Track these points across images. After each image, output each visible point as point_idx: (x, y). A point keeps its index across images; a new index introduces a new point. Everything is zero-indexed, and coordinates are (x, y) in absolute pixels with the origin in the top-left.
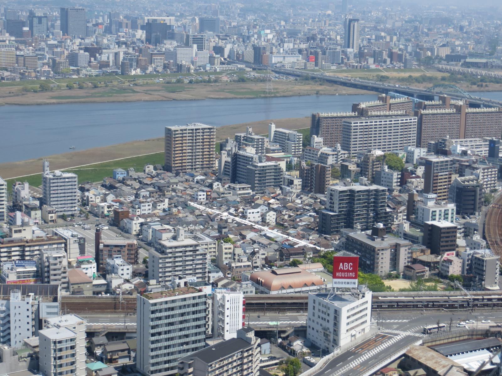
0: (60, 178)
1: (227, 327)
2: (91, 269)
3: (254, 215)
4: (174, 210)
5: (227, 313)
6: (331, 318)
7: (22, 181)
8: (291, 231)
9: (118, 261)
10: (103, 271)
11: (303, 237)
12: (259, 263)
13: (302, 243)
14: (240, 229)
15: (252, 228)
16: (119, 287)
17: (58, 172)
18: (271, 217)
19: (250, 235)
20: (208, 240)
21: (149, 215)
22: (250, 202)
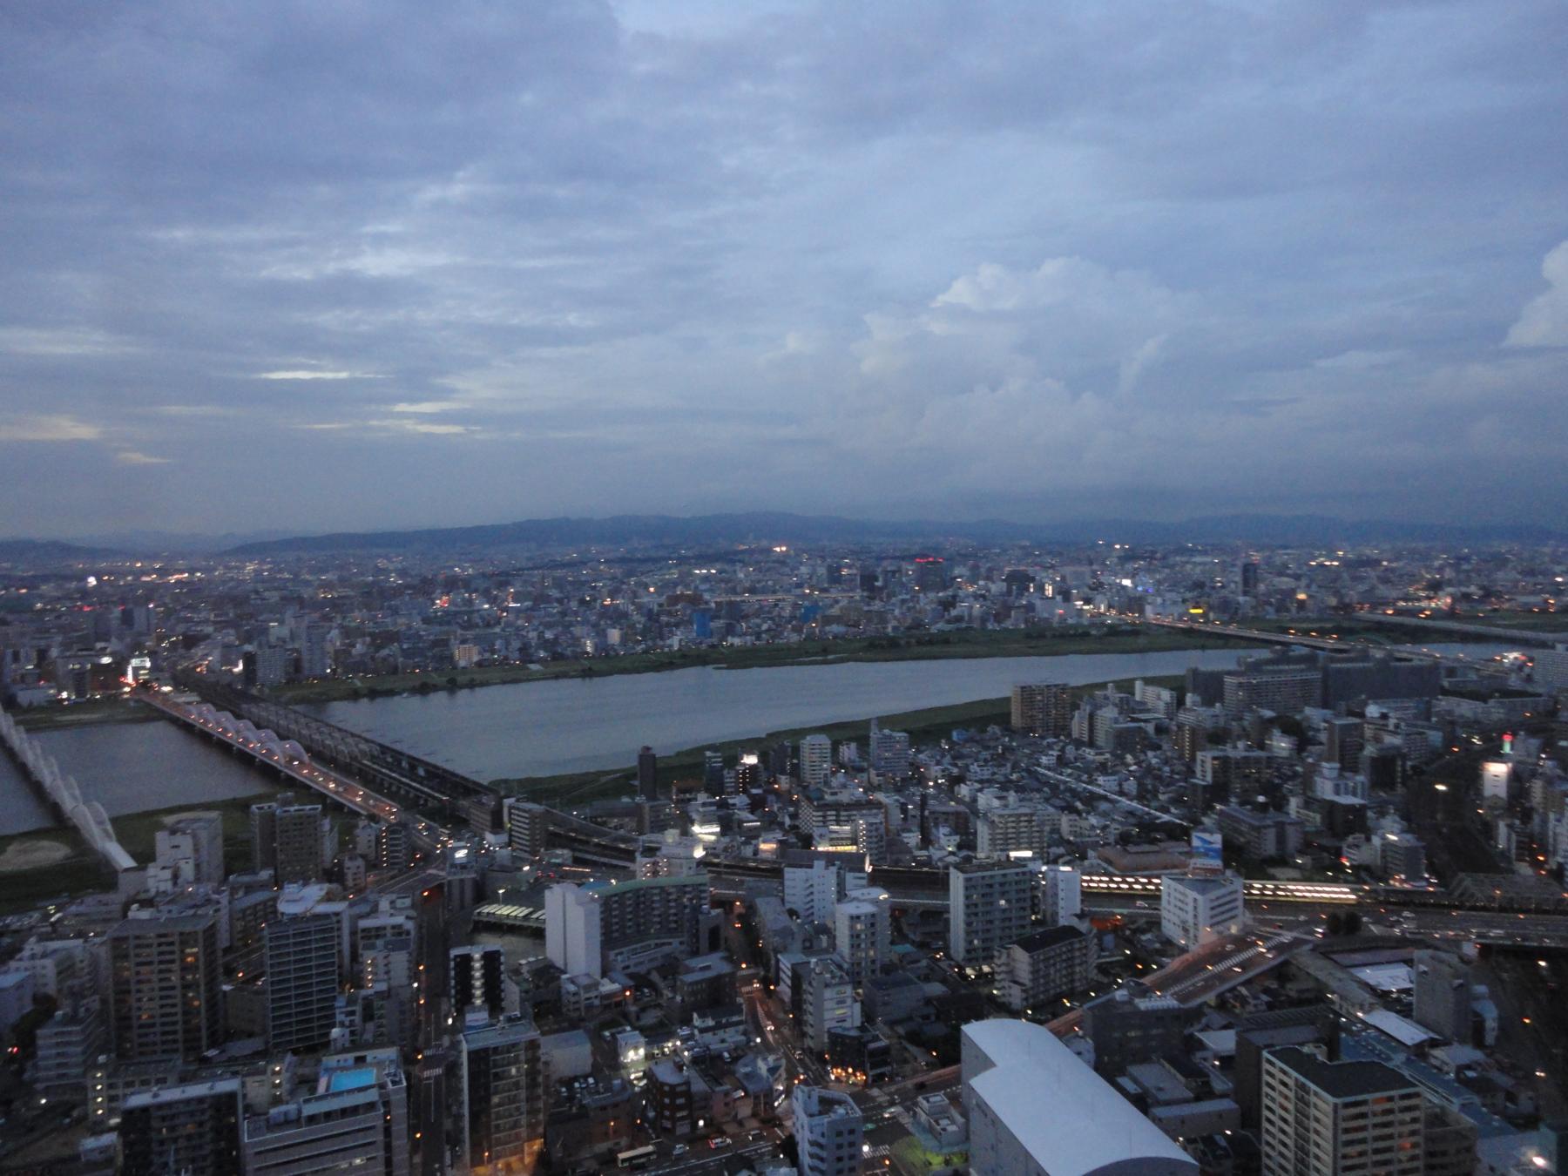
0: (890, 737)
1: (1061, 913)
2: (913, 838)
3: (1104, 784)
4: (1014, 777)
5: (1061, 894)
6: (1190, 908)
7: (850, 740)
8: (1154, 804)
9: (943, 830)
10: (926, 841)
11: (1167, 811)
12: (1111, 839)
13: (1166, 818)
14: (1091, 800)
15: (1105, 798)
16: (941, 859)
17: (886, 731)
18: (1131, 785)
19: (1104, 806)
20: (1051, 810)
21: (988, 781)
22: (1103, 768)
